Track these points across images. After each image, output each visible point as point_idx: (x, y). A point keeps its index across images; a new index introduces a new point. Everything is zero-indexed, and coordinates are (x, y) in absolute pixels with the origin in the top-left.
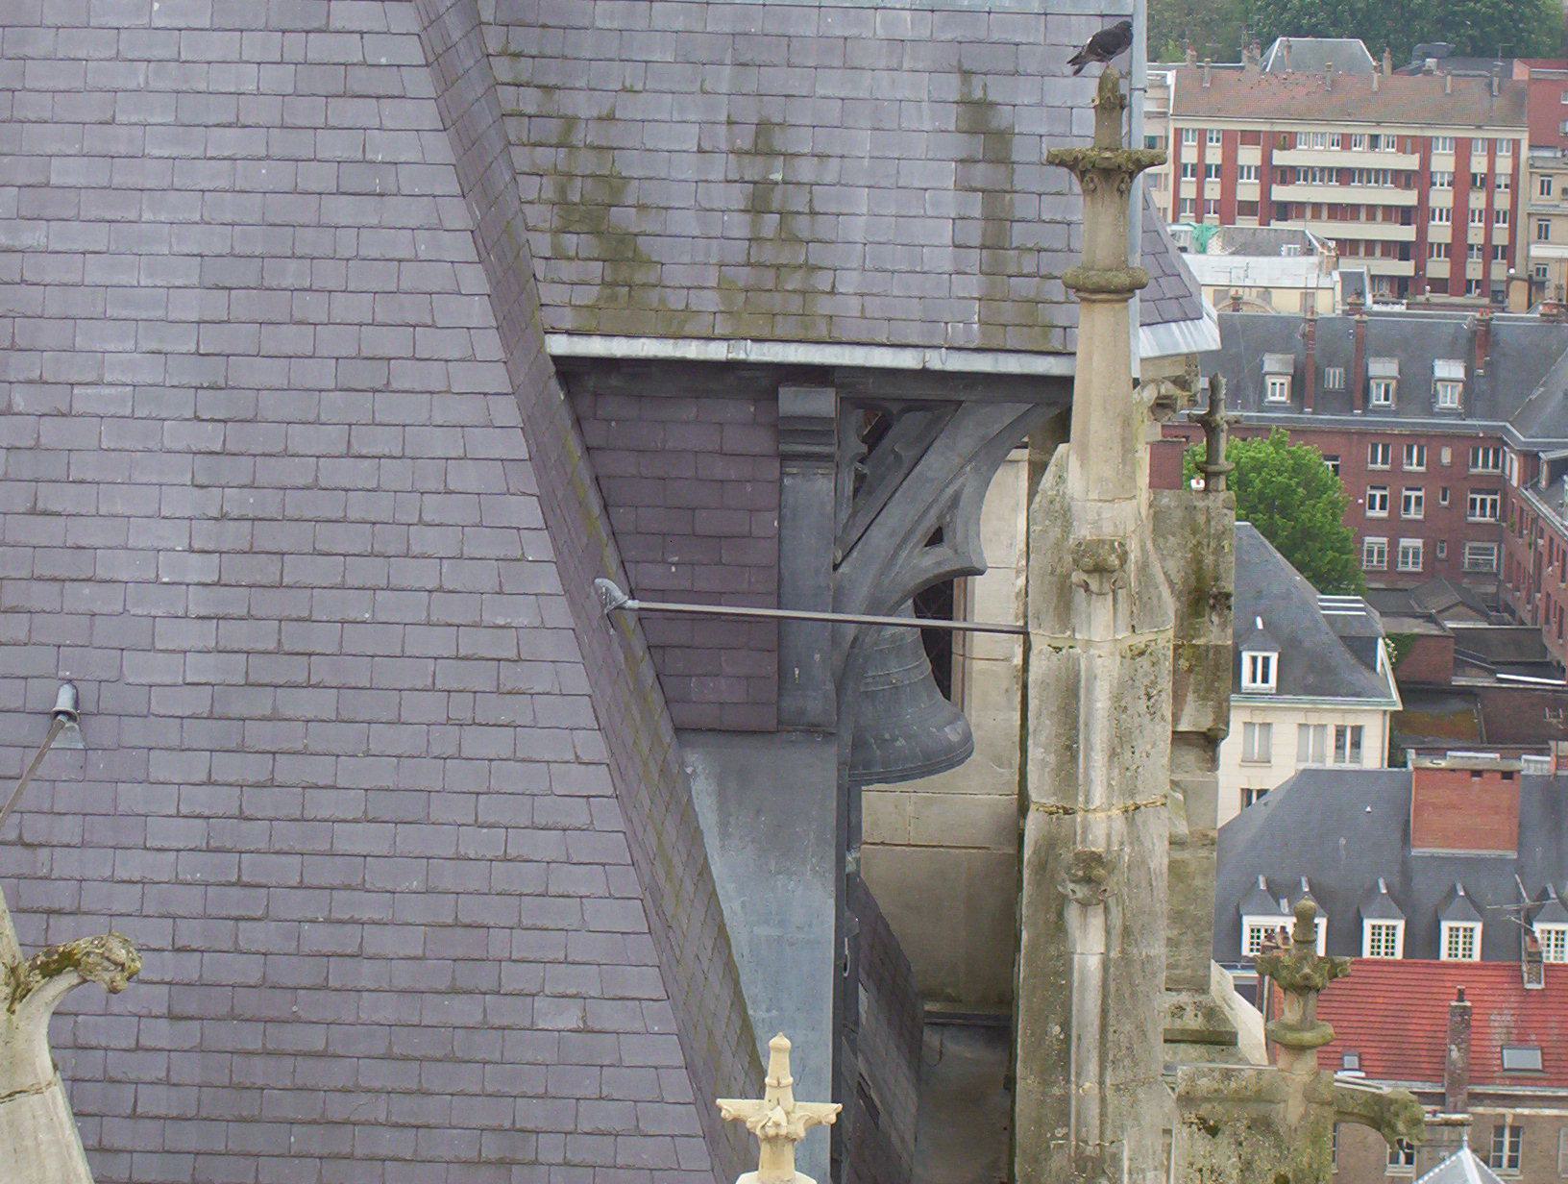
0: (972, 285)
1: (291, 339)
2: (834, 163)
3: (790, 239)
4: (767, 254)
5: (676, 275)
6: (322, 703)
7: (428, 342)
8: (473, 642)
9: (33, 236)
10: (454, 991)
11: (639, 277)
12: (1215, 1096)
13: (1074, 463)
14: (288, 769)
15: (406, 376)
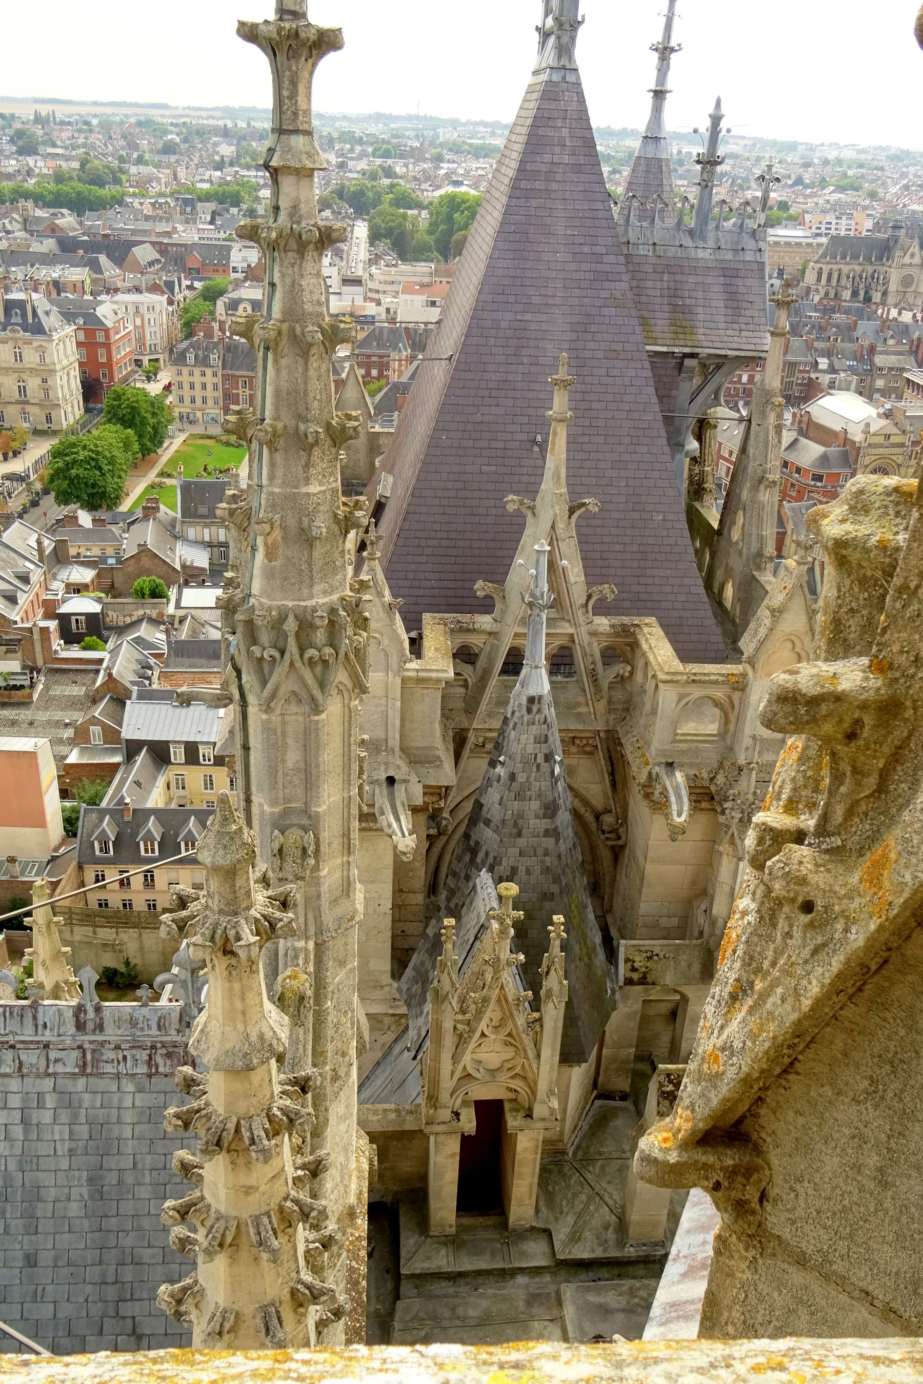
6: (601, 439)
9: (528, 317)
10: (633, 510)
14: (592, 456)
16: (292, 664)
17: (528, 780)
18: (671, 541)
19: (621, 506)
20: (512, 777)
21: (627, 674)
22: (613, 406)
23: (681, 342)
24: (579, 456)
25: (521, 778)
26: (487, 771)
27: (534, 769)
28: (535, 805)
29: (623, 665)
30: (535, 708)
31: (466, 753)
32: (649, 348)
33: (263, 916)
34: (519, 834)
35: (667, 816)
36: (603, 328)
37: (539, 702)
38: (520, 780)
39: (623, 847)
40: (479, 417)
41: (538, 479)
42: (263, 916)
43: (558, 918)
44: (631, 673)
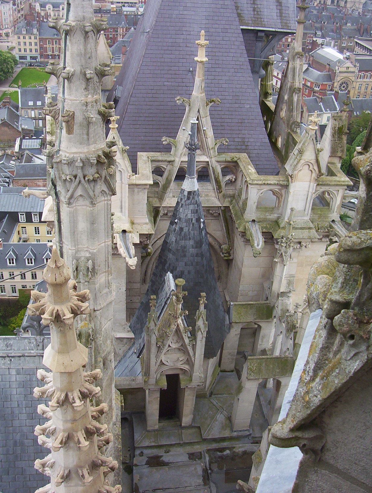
0: (279, 21)
1: (216, 26)
2: (262, 6)
3: (258, 15)
4: (256, 16)
5: (246, 19)
7: (232, 27)
8: (238, 63)
9: (185, 13)
11: (242, 19)
12: (336, 116)
13: (296, 43)
14: (216, 78)
15: (229, 31)
16: (80, 182)
17: (189, 230)
18: (253, 117)
19: (230, 101)
20: (181, 229)
21: (233, 180)
22: (226, 54)
24: (210, 77)
25: (186, 230)
26: (169, 226)
27: (191, 225)
28: (191, 242)
29: (232, 176)
31: (159, 218)
32: (242, 27)
33: (75, 305)
34: (185, 256)
35: (252, 246)
36: (220, 18)
39: (232, 260)
40: (163, 60)
41: (191, 88)
42: (75, 305)
43: (203, 294)
44: (235, 180)
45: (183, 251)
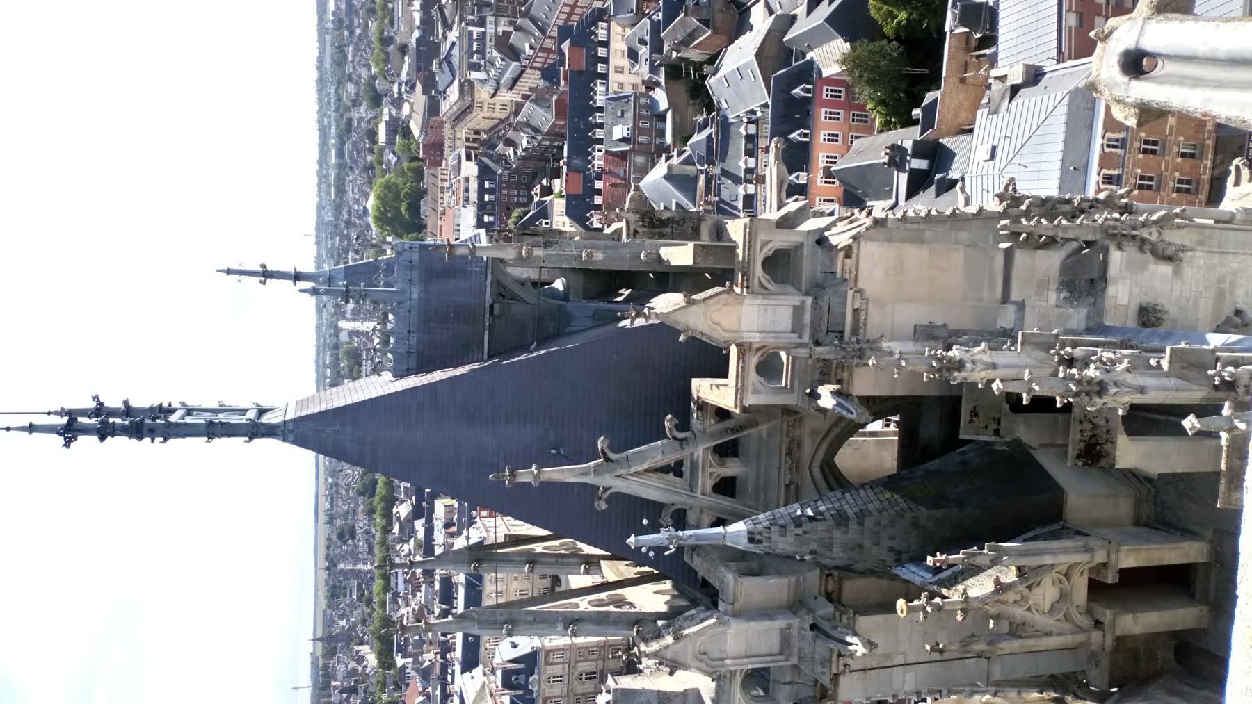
17: (815, 541)
23: (482, 318)
25: (814, 546)
27: (807, 535)
28: (837, 534)
30: (758, 537)
37: (753, 534)
38: (816, 548)
45: (852, 549)
